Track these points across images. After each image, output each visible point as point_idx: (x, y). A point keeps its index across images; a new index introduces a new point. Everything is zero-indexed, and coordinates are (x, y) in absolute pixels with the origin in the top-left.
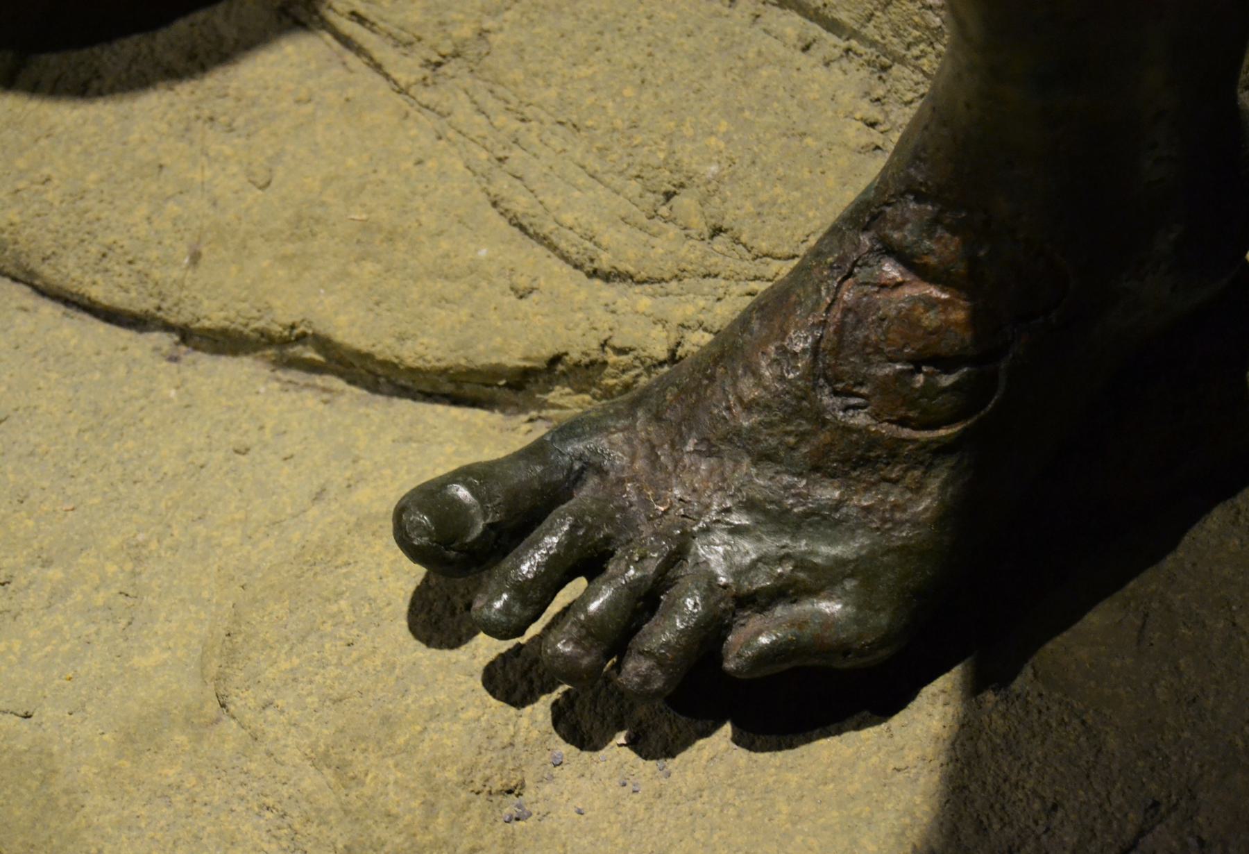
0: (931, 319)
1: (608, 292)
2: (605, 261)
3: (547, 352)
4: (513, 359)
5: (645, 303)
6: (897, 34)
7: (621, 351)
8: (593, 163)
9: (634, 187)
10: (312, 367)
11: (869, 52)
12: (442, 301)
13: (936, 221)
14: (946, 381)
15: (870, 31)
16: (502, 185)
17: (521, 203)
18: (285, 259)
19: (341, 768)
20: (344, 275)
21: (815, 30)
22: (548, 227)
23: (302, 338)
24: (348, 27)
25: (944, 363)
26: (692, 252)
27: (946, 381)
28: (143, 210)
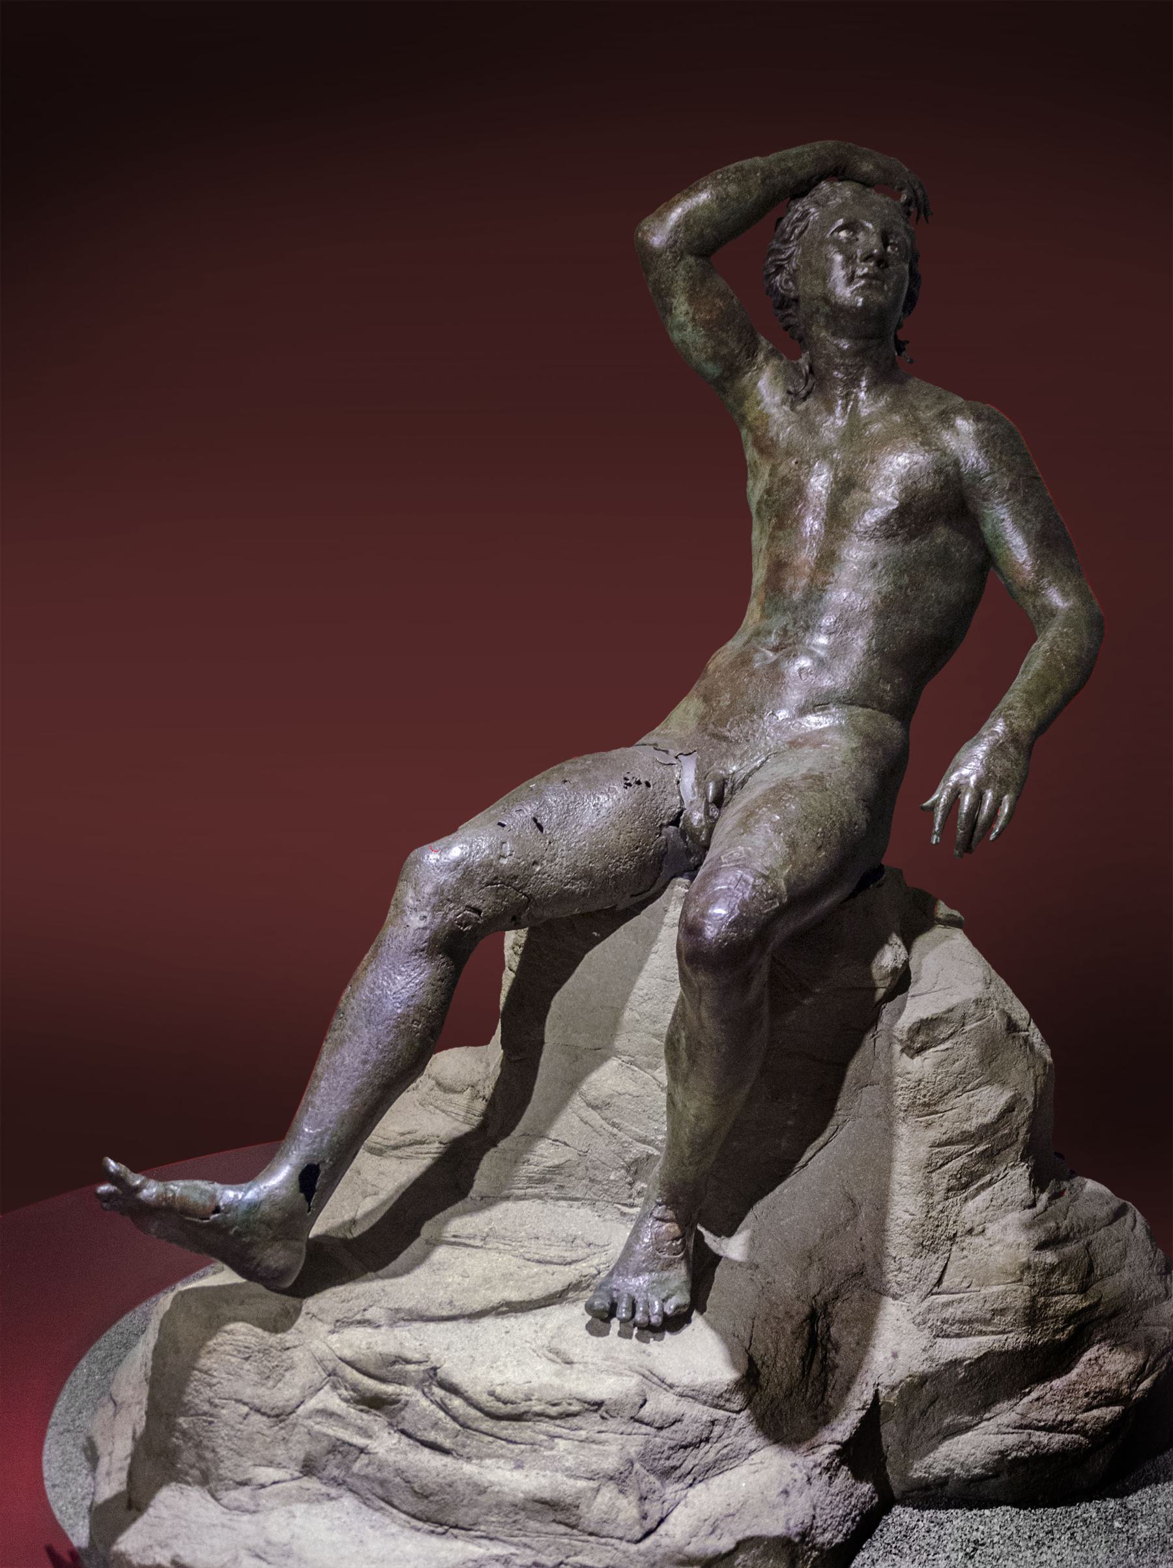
0: (672, 1230)
1: (573, 1267)
2: (569, 1260)
3: (568, 1283)
4: (560, 1288)
5: (584, 1265)
6: (595, 1194)
7: (585, 1276)
8: (547, 1242)
9: (563, 1243)
10: (504, 1313)
11: (588, 1202)
12: (534, 1283)
13: (667, 1209)
14: (679, 1243)
15: (587, 1196)
16: (527, 1256)
17: (537, 1257)
18: (487, 1289)
19: (612, 1358)
20: (506, 1286)
21: (571, 1202)
22: (549, 1258)
23: (502, 1306)
24: (453, 1240)
25: (677, 1239)
26: (587, 1250)
27: (679, 1243)
28: (442, 1293)
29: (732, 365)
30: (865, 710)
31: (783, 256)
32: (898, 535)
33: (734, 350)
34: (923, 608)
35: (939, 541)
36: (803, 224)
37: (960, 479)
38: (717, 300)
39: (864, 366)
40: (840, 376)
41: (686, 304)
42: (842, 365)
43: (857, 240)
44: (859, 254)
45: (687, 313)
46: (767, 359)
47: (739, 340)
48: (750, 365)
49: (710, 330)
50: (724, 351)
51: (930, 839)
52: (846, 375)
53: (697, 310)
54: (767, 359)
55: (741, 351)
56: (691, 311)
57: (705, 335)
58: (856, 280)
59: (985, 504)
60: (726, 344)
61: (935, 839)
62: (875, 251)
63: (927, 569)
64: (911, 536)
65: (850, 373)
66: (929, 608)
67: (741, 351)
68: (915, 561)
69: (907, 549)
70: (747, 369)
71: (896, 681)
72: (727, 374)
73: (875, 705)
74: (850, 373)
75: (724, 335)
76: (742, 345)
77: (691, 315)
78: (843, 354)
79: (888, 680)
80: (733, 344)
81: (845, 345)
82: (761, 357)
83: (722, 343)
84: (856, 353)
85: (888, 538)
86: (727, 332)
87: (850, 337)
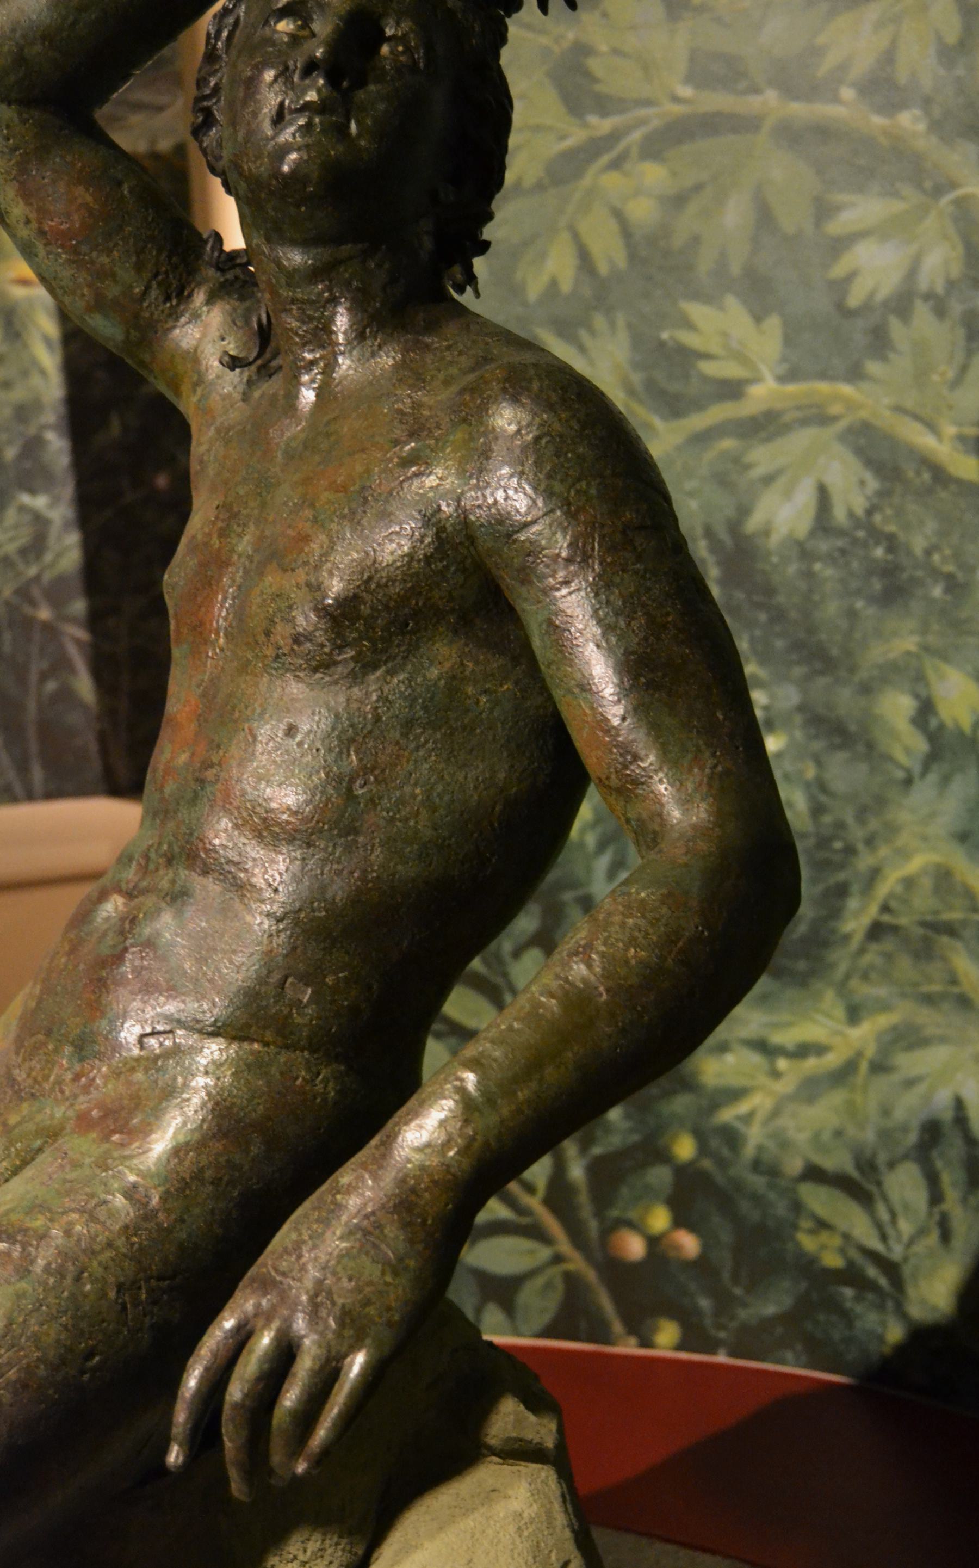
29: (136, 316)
30: (246, 1045)
31: (208, 92)
32: (336, 663)
33: (131, 287)
34: (392, 820)
35: (434, 673)
36: (231, 20)
37: (471, 539)
38: (80, 191)
39: (334, 301)
40: (295, 324)
41: (21, 203)
42: (293, 301)
43: (313, 35)
44: (299, 66)
45: (28, 222)
46: (210, 301)
47: (139, 267)
48: (174, 315)
49: (75, 251)
50: (113, 291)
51: (165, 1451)
52: (303, 322)
53: (43, 213)
54: (210, 301)
55: (148, 288)
56: (33, 216)
57: (69, 261)
58: (287, 117)
59: (523, 590)
60: (113, 276)
61: (174, 1456)
62: (319, 53)
63: (405, 735)
64: (365, 666)
65: (311, 319)
66: (407, 820)
67: (148, 288)
68: (377, 719)
69: (356, 691)
70: (170, 324)
71: (330, 980)
72: (134, 334)
73: (269, 1035)
74: (311, 319)
75: (104, 260)
76: (146, 275)
77: (34, 225)
78: (292, 277)
79: (305, 979)
80: (126, 274)
81: (296, 258)
82: (199, 297)
83: (103, 274)
84: (314, 274)
85: (315, 670)
86: (109, 252)
87: (294, 243)
